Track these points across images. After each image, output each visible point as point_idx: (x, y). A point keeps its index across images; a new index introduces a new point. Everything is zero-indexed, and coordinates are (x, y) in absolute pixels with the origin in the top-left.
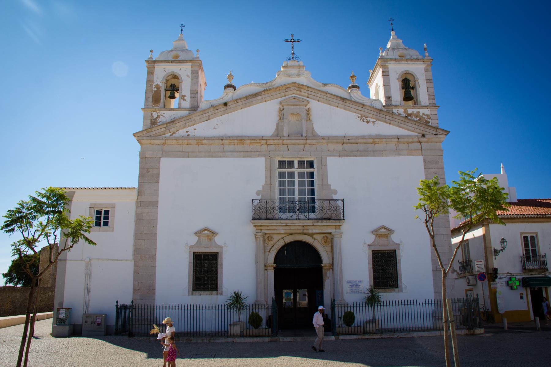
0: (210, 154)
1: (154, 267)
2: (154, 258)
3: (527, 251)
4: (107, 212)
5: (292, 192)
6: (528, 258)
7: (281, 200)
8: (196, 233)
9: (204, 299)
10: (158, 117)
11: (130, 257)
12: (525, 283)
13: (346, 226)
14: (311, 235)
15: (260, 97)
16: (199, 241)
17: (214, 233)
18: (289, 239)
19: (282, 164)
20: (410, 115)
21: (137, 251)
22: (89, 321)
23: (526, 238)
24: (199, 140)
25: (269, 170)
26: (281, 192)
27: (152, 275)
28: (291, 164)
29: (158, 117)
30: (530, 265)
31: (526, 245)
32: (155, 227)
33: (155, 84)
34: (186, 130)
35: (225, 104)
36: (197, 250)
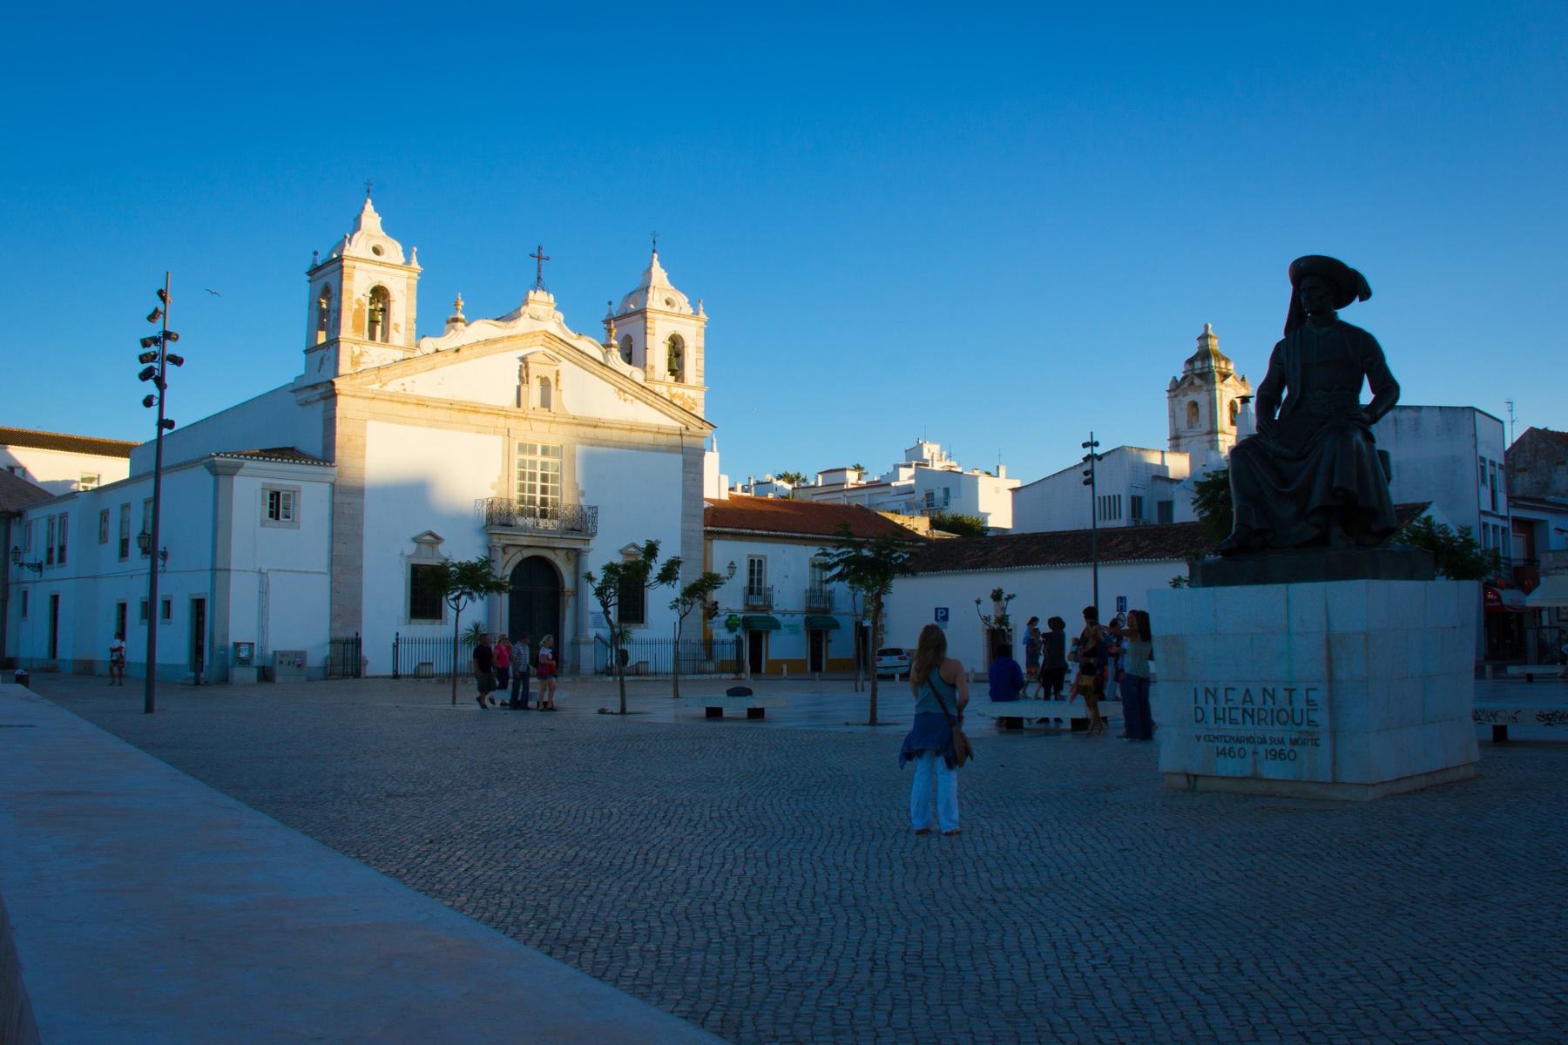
0: (434, 423)
1: (360, 584)
2: (359, 570)
3: (752, 581)
4: (288, 497)
5: (532, 489)
6: (751, 590)
7: (522, 501)
8: (415, 540)
9: (426, 629)
10: (361, 354)
11: (325, 570)
12: (746, 622)
13: (593, 543)
14: (553, 549)
15: (499, 346)
16: (419, 549)
17: (438, 539)
18: (527, 553)
19: (522, 448)
20: (673, 396)
21: (333, 560)
22: (286, 660)
23: (752, 562)
24: (421, 403)
25: (508, 456)
26: (522, 488)
27: (357, 597)
28: (533, 450)
29: (361, 354)
30: (757, 601)
31: (752, 572)
32: (360, 525)
33: (355, 297)
34: (401, 381)
35: (457, 350)
36: (416, 561)
